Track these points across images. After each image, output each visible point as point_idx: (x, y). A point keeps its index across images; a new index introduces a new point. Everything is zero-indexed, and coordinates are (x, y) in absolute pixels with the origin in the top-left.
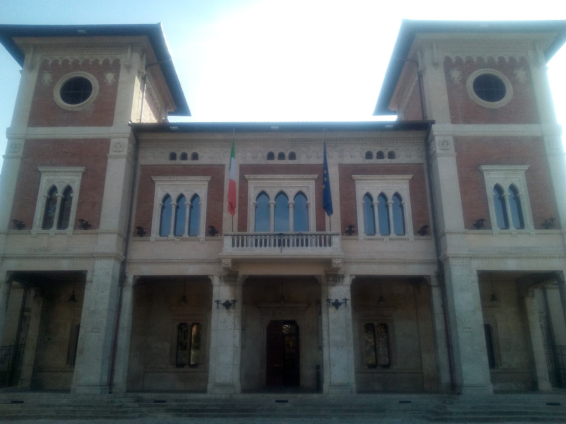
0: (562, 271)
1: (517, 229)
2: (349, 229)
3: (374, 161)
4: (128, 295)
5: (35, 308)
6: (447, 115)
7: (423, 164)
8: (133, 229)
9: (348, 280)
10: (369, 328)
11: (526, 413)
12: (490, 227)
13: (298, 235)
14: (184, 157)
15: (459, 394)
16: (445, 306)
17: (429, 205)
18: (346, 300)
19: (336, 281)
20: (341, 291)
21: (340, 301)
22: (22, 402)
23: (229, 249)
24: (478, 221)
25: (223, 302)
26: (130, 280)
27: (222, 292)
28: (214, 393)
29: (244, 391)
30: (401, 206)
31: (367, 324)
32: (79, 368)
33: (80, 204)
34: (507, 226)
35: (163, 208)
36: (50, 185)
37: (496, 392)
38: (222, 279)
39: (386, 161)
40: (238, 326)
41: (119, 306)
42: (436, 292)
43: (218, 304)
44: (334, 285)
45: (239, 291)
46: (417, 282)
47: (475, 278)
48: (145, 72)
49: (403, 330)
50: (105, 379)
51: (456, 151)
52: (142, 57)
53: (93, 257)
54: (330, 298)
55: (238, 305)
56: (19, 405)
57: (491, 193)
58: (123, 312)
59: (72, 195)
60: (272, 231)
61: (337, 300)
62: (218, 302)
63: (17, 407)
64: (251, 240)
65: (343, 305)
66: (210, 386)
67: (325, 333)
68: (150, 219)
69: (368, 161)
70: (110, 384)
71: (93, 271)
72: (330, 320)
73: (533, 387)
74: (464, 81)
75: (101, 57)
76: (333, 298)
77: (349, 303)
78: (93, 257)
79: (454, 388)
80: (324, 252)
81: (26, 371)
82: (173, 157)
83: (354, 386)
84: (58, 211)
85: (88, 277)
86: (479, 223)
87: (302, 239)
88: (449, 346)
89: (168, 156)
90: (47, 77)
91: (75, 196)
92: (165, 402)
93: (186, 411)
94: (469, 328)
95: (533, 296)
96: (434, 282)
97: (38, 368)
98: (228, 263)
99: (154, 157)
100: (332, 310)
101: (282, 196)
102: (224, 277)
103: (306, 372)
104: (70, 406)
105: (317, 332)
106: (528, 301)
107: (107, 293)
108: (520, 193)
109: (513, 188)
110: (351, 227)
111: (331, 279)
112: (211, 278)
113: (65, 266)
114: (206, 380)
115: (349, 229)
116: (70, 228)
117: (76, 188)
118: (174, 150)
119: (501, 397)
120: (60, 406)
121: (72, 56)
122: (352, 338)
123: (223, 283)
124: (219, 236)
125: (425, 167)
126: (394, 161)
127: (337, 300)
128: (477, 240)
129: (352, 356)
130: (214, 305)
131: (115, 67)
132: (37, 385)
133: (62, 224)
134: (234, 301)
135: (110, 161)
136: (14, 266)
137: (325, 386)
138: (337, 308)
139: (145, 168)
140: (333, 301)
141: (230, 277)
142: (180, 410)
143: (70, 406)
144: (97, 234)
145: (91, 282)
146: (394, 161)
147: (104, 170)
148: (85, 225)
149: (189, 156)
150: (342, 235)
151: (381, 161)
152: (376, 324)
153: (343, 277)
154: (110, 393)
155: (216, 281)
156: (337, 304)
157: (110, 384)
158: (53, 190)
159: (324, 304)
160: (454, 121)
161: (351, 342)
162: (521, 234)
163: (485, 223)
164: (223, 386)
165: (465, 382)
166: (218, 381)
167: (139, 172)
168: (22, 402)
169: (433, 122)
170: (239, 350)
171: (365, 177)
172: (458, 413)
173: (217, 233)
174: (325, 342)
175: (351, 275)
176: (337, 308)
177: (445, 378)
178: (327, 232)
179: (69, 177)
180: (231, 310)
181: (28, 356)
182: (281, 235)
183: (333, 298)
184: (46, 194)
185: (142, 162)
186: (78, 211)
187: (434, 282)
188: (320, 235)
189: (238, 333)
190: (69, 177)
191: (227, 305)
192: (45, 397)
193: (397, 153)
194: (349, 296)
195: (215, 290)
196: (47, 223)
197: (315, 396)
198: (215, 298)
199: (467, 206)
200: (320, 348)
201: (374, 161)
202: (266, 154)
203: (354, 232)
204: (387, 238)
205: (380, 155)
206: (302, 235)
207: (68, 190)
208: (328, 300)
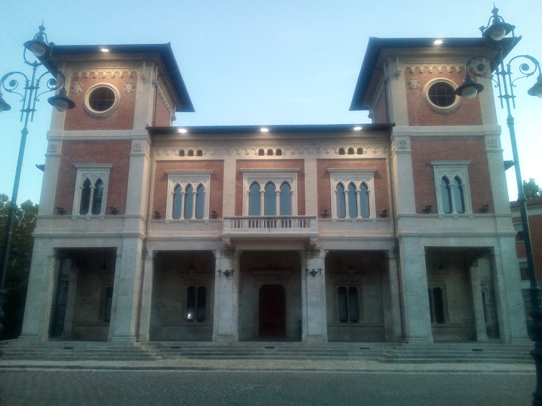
0: (493, 247)
1: (459, 213)
4: (149, 266)
5: (72, 275)
6: (406, 119)
7: (385, 159)
8: (151, 213)
10: (342, 291)
11: (455, 357)
12: (437, 212)
13: (283, 218)
15: (407, 343)
16: (399, 274)
17: (389, 192)
18: (320, 270)
19: (313, 255)
20: (317, 263)
21: (316, 270)
22: (72, 348)
23: (229, 230)
24: (427, 207)
25: (223, 271)
26: (150, 255)
27: (223, 264)
28: (217, 341)
29: (241, 340)
30: (367, 193)
31: (340, 288)
33: (109, 194)
34: (451, 211)
35: (175, 195)
36: (85, 178)
37: (435, 342)
38: (223, 253)
40: (236, 290)
42: (392, 264)
43: (220, 273)
44: (312, 258)
45: (237, 263)
47: (423, 252)
48: (157, 82)
49: (368, 294)
51: (412, 149)
52: (154, 70)
53: (121, 236)
54: (308, 268)
55: (236, 273)
56: (70, 350)
58: (145, 278)
59: (102, 186)
60: (262, 214)
61: (313, 270)
62: (220, 271)
63: (69, 352)
64: (246, 222)
65: (318, 274)
66: (214, 336)
67: (304, 295)
68: (164, 206)
71: (122, 247)
72: (308, 285)
73: (472, 337)
76: (310, 268)
77: (323, 272)
78: (122, 237)
79: (403, 338)
80: (304, 232)
81: (68, 326)
83: (326, 336)
84: (91, 200)
85: (118, 252)
86: (427, 209)
87: (286, 221)
88: (401, 306)
91: (105, 187)
92: (180, 348)
93: (196, 355)
94: (417, 292)
95: (476, 266)
98: (227, 241)
100: (309, 277)
101: (270, 185)
102: (224, 252)
103: (291, 325)
104: (109, 351)
105: (299, 294)
106: (472, 269)
108: (463, 184)
109: (457, 179)
110: (325, 211)
111: (309, 253)
112: (214, 252)
113: (99, 244)
114: (211, 331)
115: (325, 213)
116: (102, 214)
117: (106, 180)
118: (182, 148)
119: (438, 345)
120: (101, 351)
122: (325, 299)
123: (224, 256)
124: (220, 219)
125: (387, 161)
127: (313, 270)
129: (325, 314)
130: (217, 274)
132: (76, 337)
133: (96, 210)
134: (233, 271)
135: (132, 159)
136: (60, 244)
137: (304, 336)
138: (314, 276)
140: (311, 270)
141: (229, 251)
142: (192, 354)
143: (109, 351)
144: (124, 218)
145: (121, 256)
147: (128, 166)
150: (319, 217)
153: (319, 251)
154: (137, 341)
155: (218, 255)
156: (313, 273)
157: (137, 335)
158: (87, 183)
159: (303, 272)
160: (412, 123)
161: (325, 302)
162: (462, 217)
163: (432, 208)
164: (225, 336)
165: (412, 334)
166: (221, 332)
168: (72, 348)
169: (394, 125)
172: (402, 357)
173: (218, 216)
174: (304, 302)
175: (325, 250)
176: (314, 276)
177: (398, 330)
178: (307, 215)
179: (99, 173)
180: (230, 277)
181: (69, 313)
182: (269, 218)
183: (310, 268)
184: (82, 187)
186: (109, 199)
187: (391, 255)
188: (301, 218)
190: (99, 173)
191: (227, 274)
192: (89, 345)
193: (364, 150)
194: (323, 267)
195: (217, 262)
196: (84, 208)
197: (296, 344)
198: (217, 269)
199: (418, 195)
200: (300, 307)
202: (257, 151)
203: (328, 215)
204: (354, 220)
206: (286, 218)
207: (99, 182)
208: (307, 270)
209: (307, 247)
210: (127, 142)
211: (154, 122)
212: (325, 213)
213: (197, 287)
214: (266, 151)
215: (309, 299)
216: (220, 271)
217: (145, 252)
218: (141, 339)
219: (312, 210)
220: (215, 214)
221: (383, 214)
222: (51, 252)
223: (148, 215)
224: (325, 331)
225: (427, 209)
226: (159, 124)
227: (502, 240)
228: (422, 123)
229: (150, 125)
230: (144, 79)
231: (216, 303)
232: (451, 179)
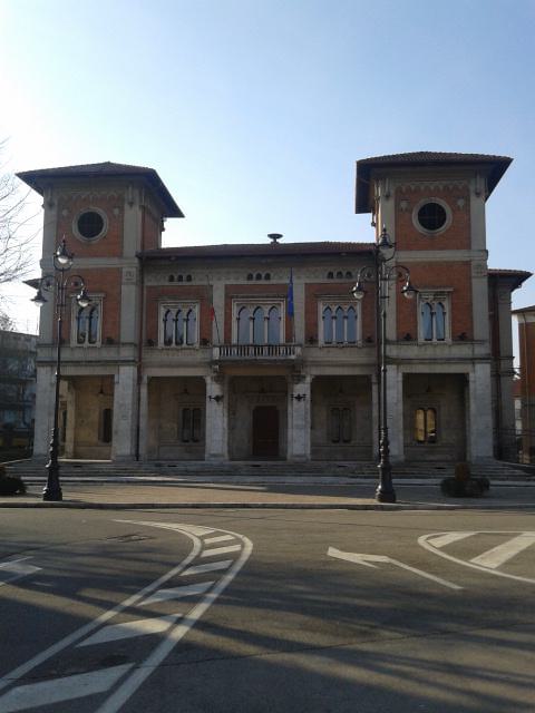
4: (144, 391)
9: (309, 379)
14: (180, 279)
20: (303, 388)
26: (145, 380)
27: (213, 389)
32: (114, 442)
40: (226, 414)
41: (139, 399)
42: (375, 388)
45: (226, 388)
46: (367, 378)
47: (400, 379)
50: (134, 452)
55: (226, 399)
69: (331, 281)
70: (137, 456)
82: (172, 279)
85: (116, 379)
89: (167, 278)
90: (65, 213)
96: (374, 380)
97: (76, 443)
99: (157, 281)
100: (295, 401)
107: (130, 392)
114: (204, 451)
130: (208, 399)
131: (119, 203)
139: (148, 287)
141: (219, 379)
148: (110, 341)
149: (184, 278)
152: (341, 408)
155: (208, 380)
156: (299, 398)
164: (214, 455)
166: (212, 452)
167: (145, 292)
170: (227, 431)
181: (70, 434)
185: (147, 283)
187: (374, 380)
189: (226, 419)
191: (218, 399)
195: (208, 388)
198: (208, 395)
202: (246, 276)
209: (295, 370)
210: (119, 270)
211: (143, 246)
212: (312, 339)
213: (192, 408)
214: (254, 276)
215: (295, 423)
216: (210, 397)
217: (140, 378)
218: (141, 458)
219: (300, 335)
220: (205, 342)
221: (368, 340)
223: (141, 342)
224: (309, 452)
226: (149, 249)
227: (478, 366)
228: (409, 248)
229: (140, 251)
230: (131, 204)
231: (208, 425)
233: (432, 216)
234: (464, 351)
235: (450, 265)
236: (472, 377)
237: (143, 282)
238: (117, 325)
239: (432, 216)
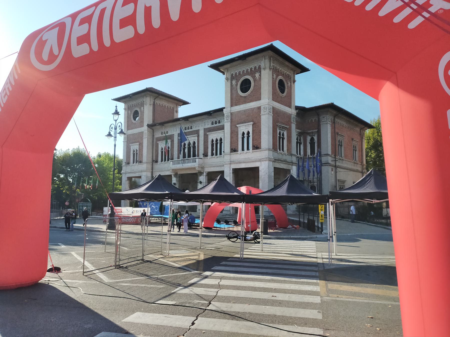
2: (205, 155)
3: (215, 125)
9: (205, 174)
39: (218, 124)
47: (231, 172)
57: (240, 136)
74: (237, 85)
75: (140, 101)
121: (134, 103)
126: (220, 124)
128: (235, 157)
131: (142, 105)
141: (176, 175)
146: (220, 124)
151: (216, 125)
167: (155, 140)
171: (210, 133)
190: (135, 147)
201: (215, 125)
205: (216, 123)
222: (126, 179)
225: (234, 150)
227: (262, 162)
229: (151, 122)
232: (246, 133)
233: (245, 86)
234: (257, 154)
235: (252, 109)
236: (260, 169)
237: (153, 136)
238: (142, 155)
239: (245, 86)
